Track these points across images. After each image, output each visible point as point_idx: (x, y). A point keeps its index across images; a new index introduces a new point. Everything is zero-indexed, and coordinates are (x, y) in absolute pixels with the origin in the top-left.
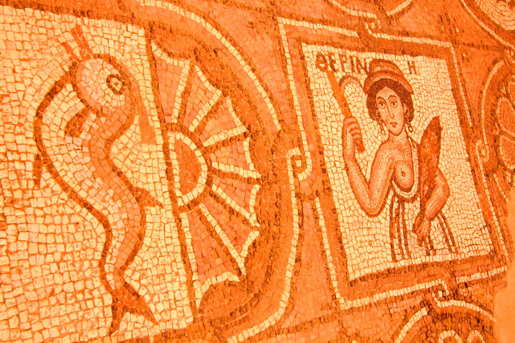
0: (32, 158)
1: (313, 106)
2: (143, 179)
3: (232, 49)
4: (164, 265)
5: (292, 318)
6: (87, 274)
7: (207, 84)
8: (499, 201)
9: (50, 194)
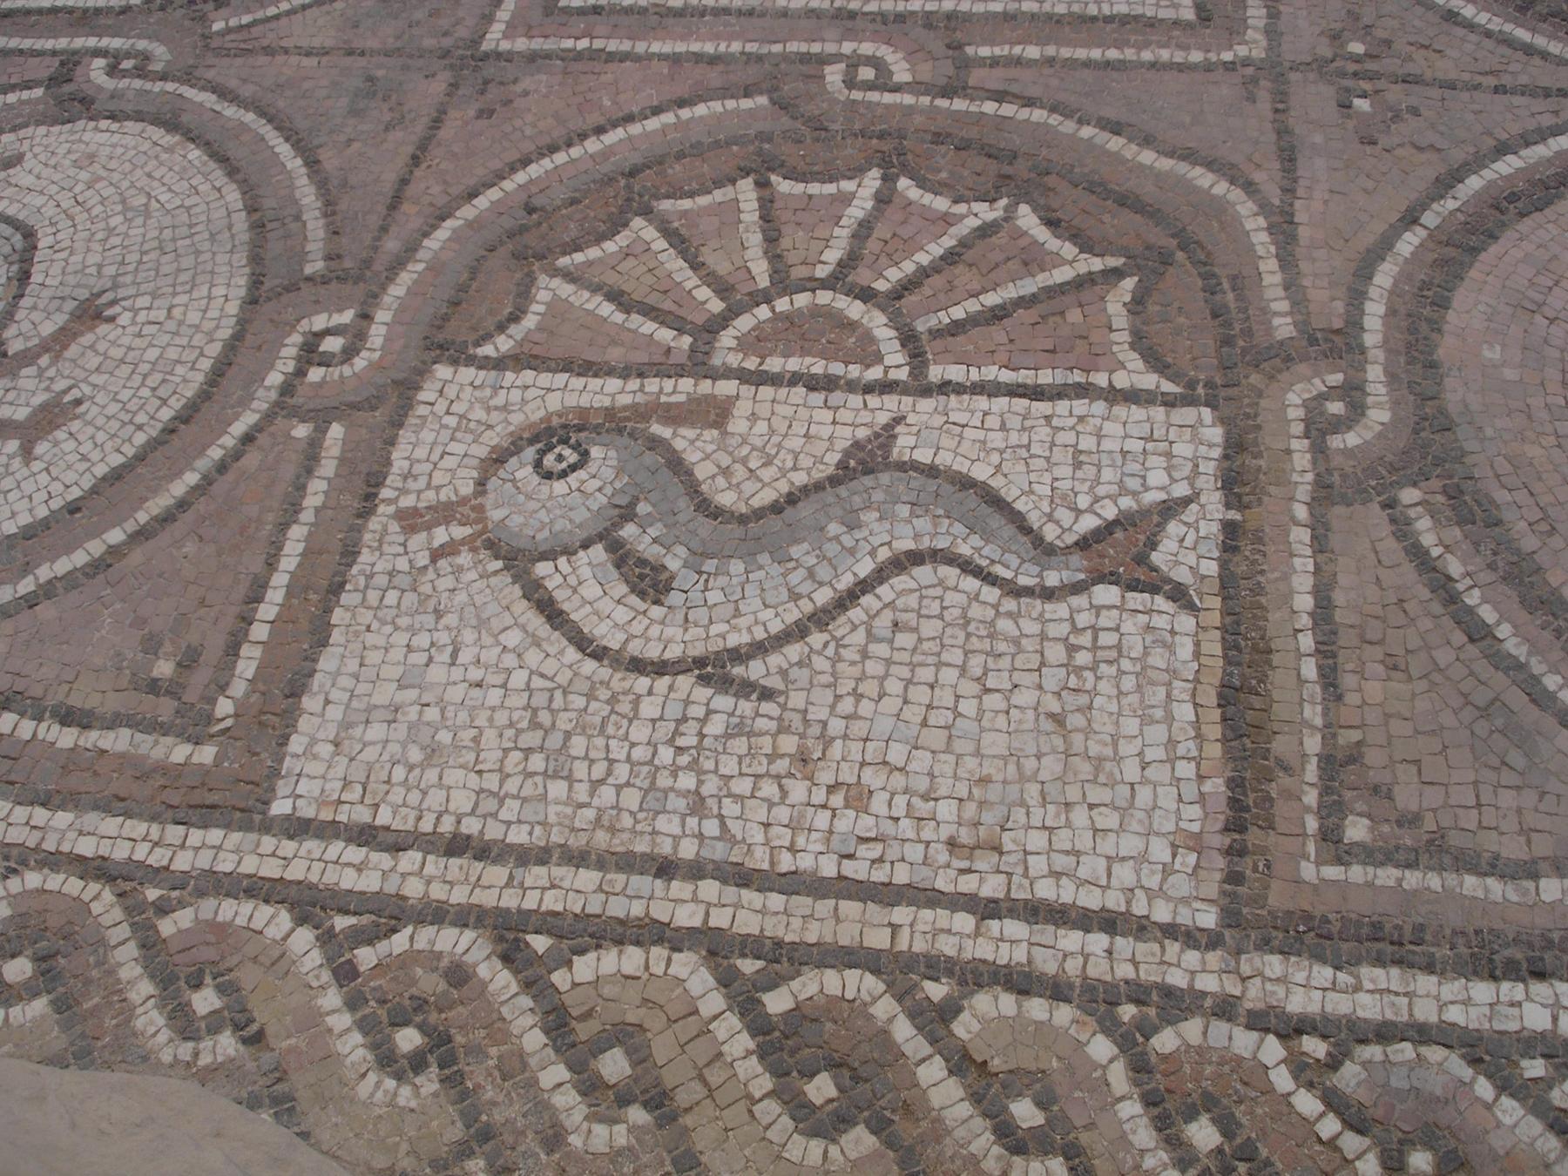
2: (819, 448)
3: (534, 170)
4: (1053, 444)
5: (1258, 177)
7: (610, 246)
9: (806, 672)
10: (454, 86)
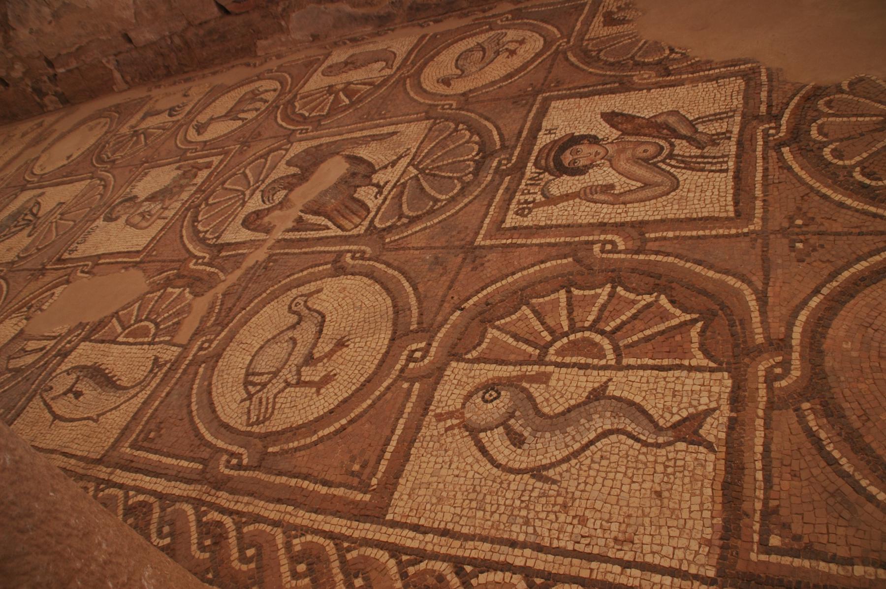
0: (532, 481)
1: (560, 226)
2: (580, 391)
3: (489, 289)
5: (754, 278)
6: (652, 459)
7: (514, 317)
8: (696, 67)
9: (568, 474)
10: (464, 259)
